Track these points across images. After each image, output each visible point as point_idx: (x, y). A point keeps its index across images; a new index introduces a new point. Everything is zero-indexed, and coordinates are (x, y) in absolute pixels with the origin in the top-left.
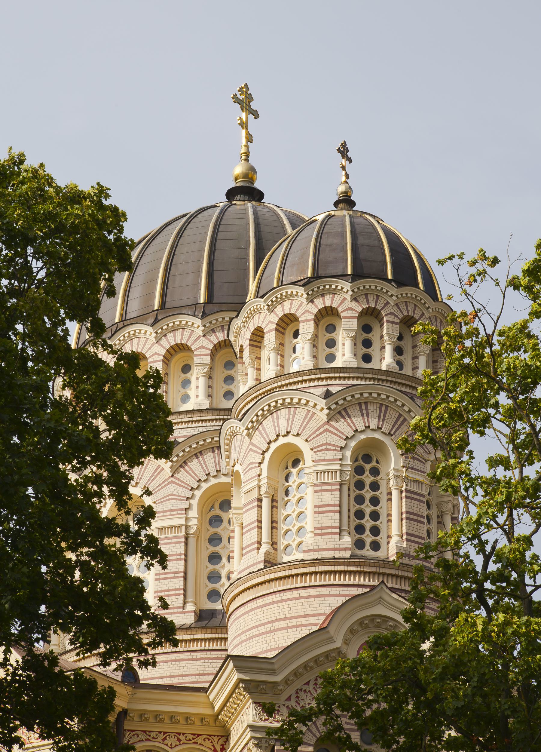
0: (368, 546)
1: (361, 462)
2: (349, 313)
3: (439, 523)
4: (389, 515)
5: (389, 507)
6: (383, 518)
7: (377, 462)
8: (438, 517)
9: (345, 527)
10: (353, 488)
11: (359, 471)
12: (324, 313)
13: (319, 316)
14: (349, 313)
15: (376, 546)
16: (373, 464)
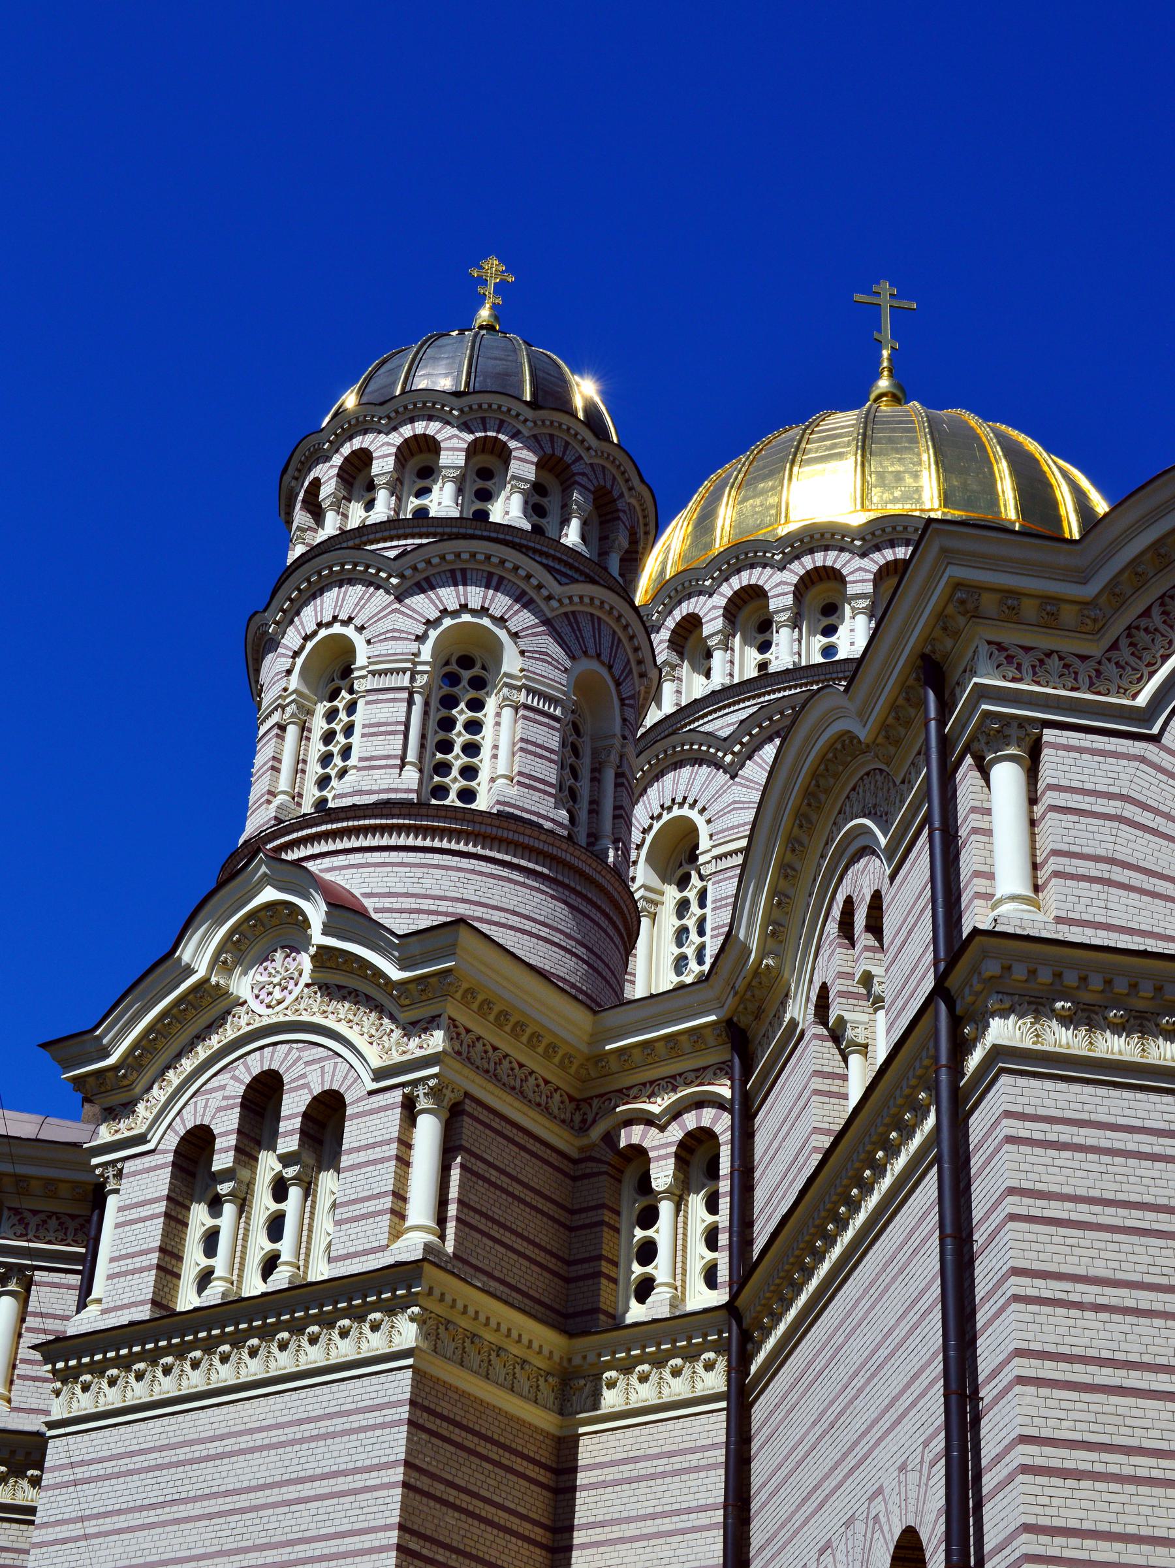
0: (453, 795)
1: (454, 667)
2: (455, 443)
3: (593, 780)
4: (496, 747)
5: (497, 735)
6: (486, 752)
7: (484, 668)
8: (593, 770)
9: (411, 756)
10: (434, 703)
11: (452, 679)
12: (414, 446)
13: (406, 452)
14: (455, 443)
15: (468, 795)
16: (476, 671)
